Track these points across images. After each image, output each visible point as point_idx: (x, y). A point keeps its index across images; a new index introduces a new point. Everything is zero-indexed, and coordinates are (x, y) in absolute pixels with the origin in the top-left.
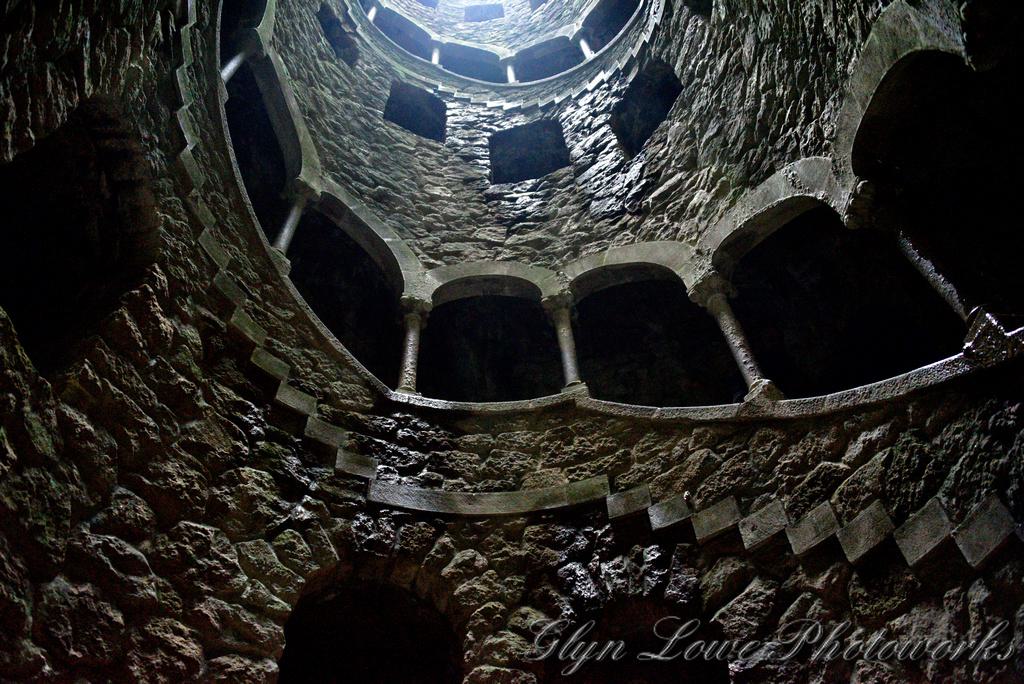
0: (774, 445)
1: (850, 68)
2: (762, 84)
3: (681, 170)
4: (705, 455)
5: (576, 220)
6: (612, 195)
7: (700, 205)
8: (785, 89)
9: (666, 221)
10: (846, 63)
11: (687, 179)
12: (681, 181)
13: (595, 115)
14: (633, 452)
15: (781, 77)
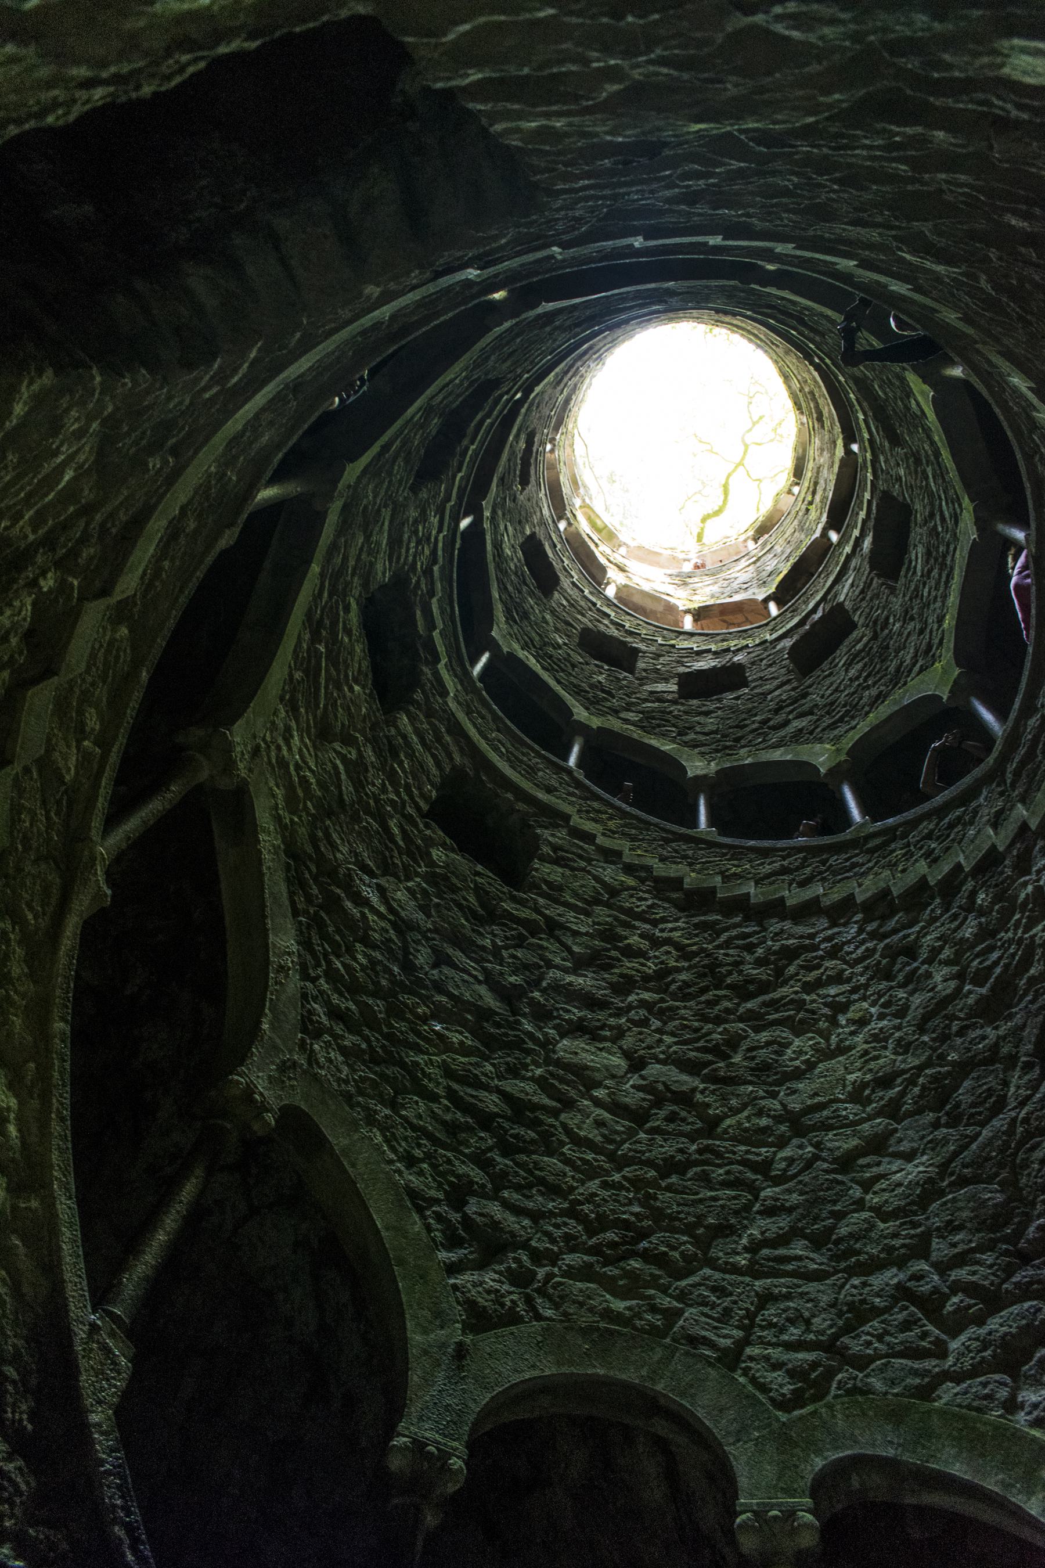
0: (35, 918)
1: (379, 1139)
2: (370, 917)
3: (326, 706)
4: (68, 778)
5: (366, 507)
6: (353, 574)
7: (290, 749)
8: (363, 968)
9: (298, 675)
10: (383, 1130)
11: (315, 717)
12: (317, 706)
13: (419, 542)
14: (124, 631)
15: (373, 962)
